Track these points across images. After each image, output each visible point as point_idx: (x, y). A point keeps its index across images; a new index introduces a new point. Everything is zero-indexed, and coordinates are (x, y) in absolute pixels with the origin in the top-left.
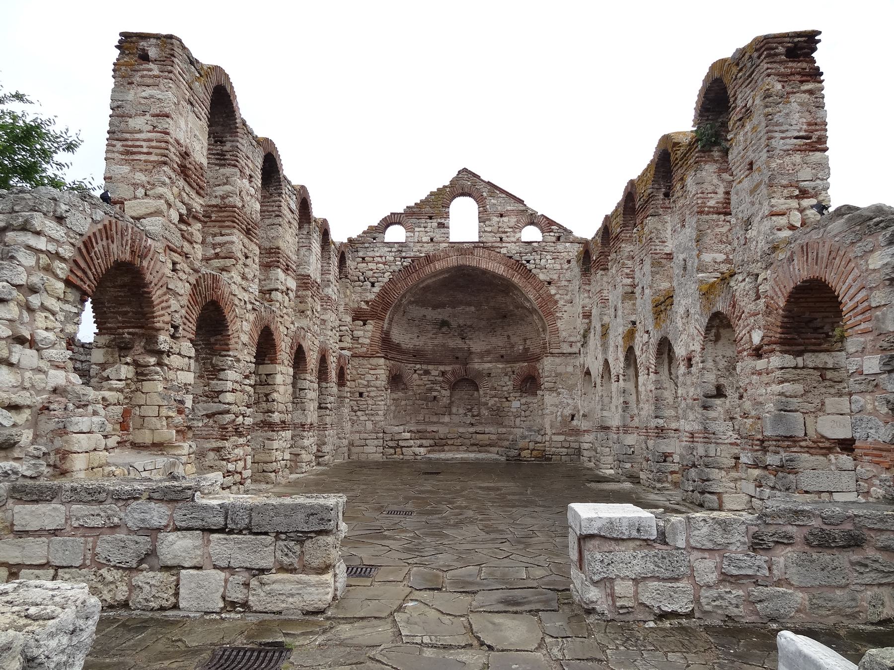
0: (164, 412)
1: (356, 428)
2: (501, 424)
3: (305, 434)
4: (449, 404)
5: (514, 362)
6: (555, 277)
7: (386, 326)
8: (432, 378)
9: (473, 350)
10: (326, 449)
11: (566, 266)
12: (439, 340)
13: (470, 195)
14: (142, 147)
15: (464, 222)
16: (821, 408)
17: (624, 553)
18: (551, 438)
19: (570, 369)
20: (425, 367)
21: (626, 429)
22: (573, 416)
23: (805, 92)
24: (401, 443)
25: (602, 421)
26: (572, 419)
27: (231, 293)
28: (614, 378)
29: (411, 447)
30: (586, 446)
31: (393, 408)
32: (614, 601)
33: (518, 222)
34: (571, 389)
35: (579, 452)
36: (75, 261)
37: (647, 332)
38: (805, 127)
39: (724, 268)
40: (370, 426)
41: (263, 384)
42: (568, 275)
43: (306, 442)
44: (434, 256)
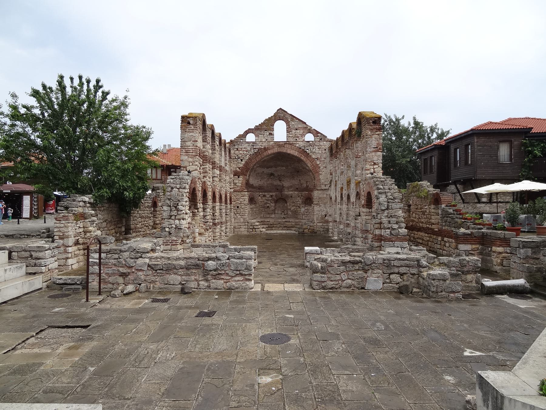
0: (201, 225)
1: (236, 221)
2: (297, 218)
6: (319, 157)
10: (228, 230)
11: (324, 152)
15: (280, 132)
19: (325, 196)
20: (263, 193)
21: (340, 223)
22: (326, 215)
24: (255, 227)
33: (303, 132)
34: (325, 204)
35: (328, 230)
40: (242, 220)
42: (325, 156)
44: (268, 148)
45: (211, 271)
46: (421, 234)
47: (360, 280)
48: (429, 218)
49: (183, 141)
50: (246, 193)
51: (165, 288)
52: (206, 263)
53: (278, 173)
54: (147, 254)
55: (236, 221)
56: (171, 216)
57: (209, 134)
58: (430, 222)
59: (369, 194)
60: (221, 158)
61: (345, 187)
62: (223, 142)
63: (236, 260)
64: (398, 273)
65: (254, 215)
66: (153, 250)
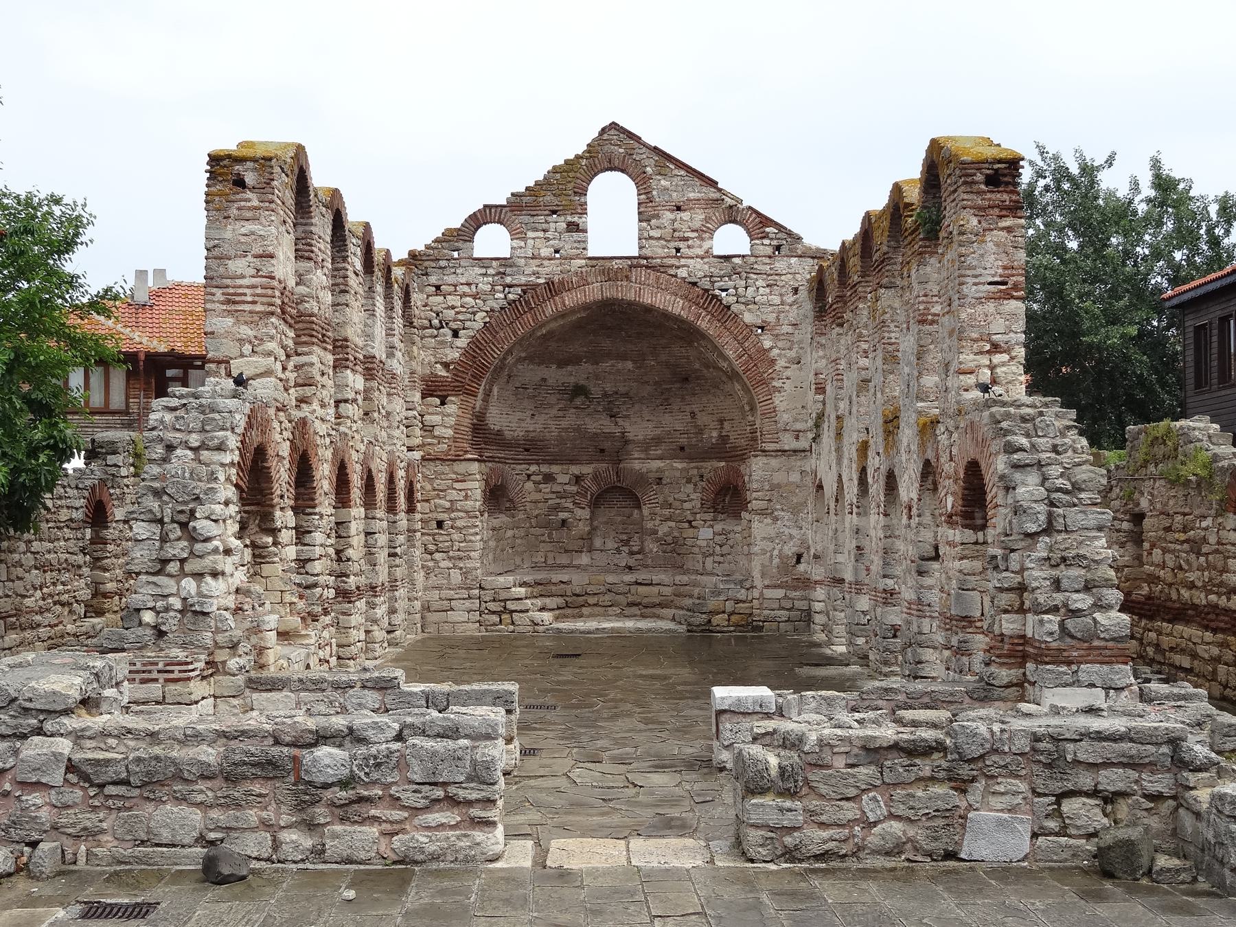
0: (288, 598)
1: (433, 581)
2: (682, 569)
3: (378, 600)
4: (589, 533)
5: (703, 459)
6: (771, 318)
7: (479, 404)
8: (559, 488)
9: (630, 436)
10: (398, 618)
11: (790, 298)
13: (623, 171)
14: (245, 295)
15: (612, 219)
18: (762, 594)
19: (795, 477)
20: (545, 469)
21: (858, 587)
23: (1002, 229)
24: (511, 606)
25: (836, 570)
26: (798, 562)
29: (527, 611)
31: (492, 544)
34: (795, 510)
35: (807, 616)
38: (1000, 271)
40: (456, 577)
42: (793, 314)
44: (562, 282)
45: (326, 786)
46: (1191, 632)
47: (941, 822)
48: (1220, 565)
49: (215, 253)
50: (475, 467)
51: (139, 861)
52: (307, 756)
53: (606, 385)
54: (65, 720)
55: (433, 581)
56: (165, 562)
57: (322, 226)
58: (1221, 584)
59: (973, 470)
60: (368, 325)
61: (877, 442)
62: (378, 258)
63: (429, 744)
64: (1094, 793)
65: (504, 554)
66: (88, 703)
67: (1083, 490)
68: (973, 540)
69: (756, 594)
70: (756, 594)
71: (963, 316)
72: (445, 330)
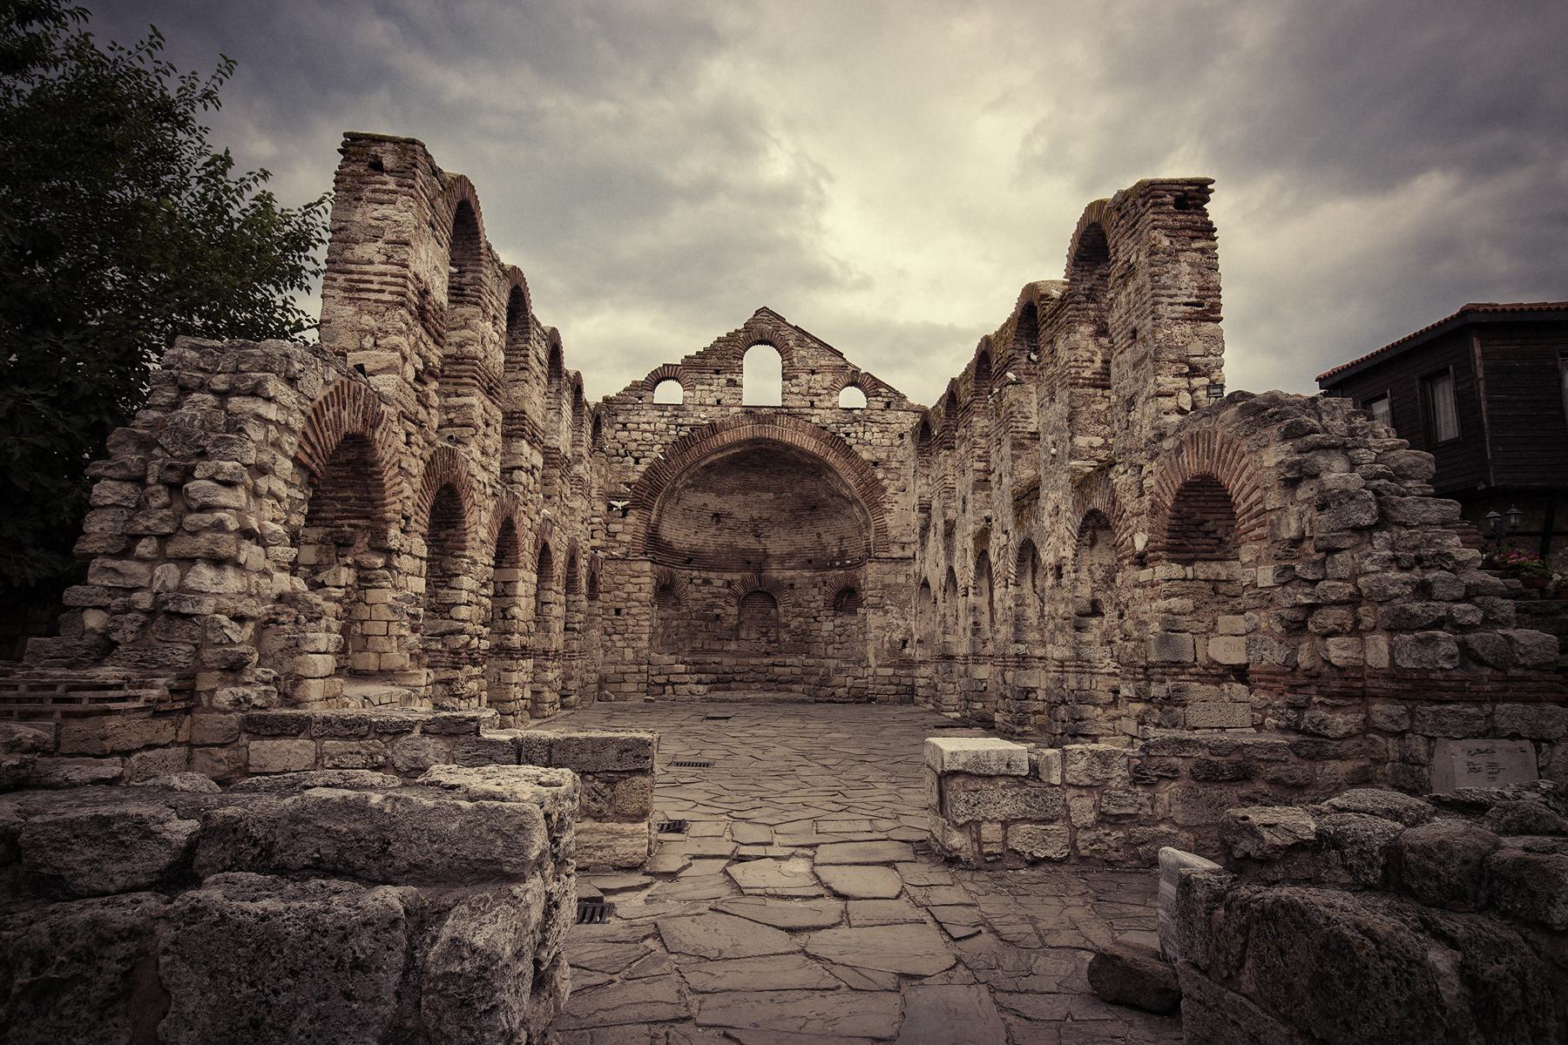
3: (549, 664)
6: (883, 456)
7: (654, 517)
9: (770, 552)
10: (572, 685)
12: (725, 538)
13: (770, 343)
14: (372, 282)
15: (762, 380)
16: (1213, 629)
17: (992, 791)
19: (901, 579)
20: (704, 574)
21: (976, 658)
22: (905, 642)
24: (672, 679)
26: (904, 646)
27: (469, 474)
28: (961, 592)
30: (922, 682)
32: (980, 848)
34: (902, 605)
36: (304, 434)
37: (1006, 532)
39: (1102, 454)
41: (503, 593)
43: (550, 676)
44: (722, 424)
67: (1411, 478)
68: (1182, 575)
69: (871, 671)
70: (871, 671)
71: (1160, 336)
72: (629, 458)
